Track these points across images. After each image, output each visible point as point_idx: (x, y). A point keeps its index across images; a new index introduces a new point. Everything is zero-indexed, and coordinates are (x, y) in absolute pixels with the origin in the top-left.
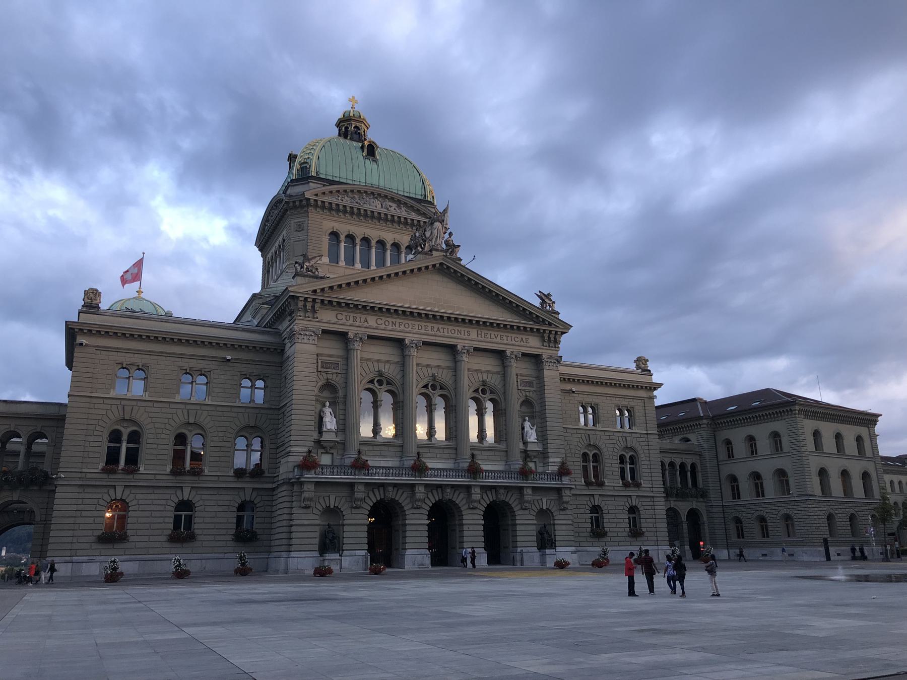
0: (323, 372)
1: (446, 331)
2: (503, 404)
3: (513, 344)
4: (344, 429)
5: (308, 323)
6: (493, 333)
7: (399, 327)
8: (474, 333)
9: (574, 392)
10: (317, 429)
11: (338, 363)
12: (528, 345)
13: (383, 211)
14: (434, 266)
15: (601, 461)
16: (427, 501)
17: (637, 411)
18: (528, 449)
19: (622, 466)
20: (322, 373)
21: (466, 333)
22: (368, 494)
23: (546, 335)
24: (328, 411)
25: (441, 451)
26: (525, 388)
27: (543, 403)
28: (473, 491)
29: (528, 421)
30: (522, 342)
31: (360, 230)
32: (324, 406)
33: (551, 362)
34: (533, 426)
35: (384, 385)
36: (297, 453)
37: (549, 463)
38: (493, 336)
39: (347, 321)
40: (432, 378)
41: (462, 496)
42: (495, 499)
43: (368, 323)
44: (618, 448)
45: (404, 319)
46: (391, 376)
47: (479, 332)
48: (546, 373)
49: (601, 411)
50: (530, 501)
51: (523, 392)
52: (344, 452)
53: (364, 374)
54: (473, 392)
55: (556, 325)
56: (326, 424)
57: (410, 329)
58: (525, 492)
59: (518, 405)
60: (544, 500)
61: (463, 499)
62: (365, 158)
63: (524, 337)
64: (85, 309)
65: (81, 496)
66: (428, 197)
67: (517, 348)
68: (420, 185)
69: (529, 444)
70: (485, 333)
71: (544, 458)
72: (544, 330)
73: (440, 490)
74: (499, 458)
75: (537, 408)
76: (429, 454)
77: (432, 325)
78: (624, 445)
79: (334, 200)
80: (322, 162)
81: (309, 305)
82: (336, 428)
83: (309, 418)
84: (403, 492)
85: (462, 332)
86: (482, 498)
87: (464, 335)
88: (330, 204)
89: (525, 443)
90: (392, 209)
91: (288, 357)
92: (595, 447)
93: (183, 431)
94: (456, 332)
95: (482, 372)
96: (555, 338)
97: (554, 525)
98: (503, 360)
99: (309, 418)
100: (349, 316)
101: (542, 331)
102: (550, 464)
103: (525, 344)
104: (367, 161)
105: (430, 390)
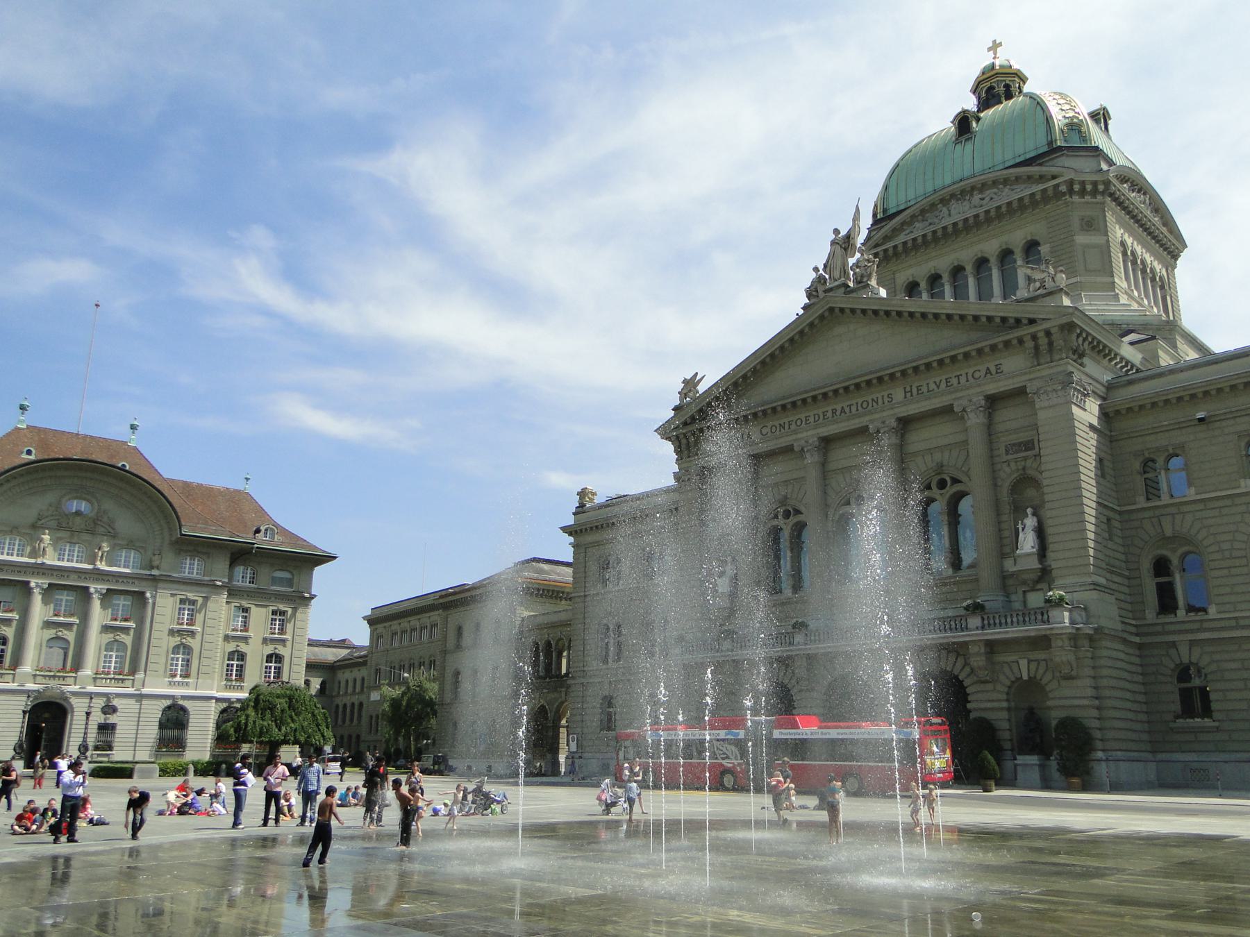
1: (854, 408)
8: (898, 394)
9: (1201, 420)
14: (822, 317)
21: (885, 397)
23: (1030, 344)
29: (1034, 514)
38: (932, 386)
47: (908, 389)
48: (1042, 415)
51: (1012, 464)
55: (1044, 319)
66: (1056, 140)
67: (978, 390)
68: (1042, 129)
70: (917, 387)
72: (1021, 341)
77: (835, 407)
79: (902, 238)
80: (892, 190)
81: (684, 441)
85: (880, 401)
88: (895, 247)
90: (984, 202)
94: (870, 405)
101: (1015, 342)
104: (959, 147)
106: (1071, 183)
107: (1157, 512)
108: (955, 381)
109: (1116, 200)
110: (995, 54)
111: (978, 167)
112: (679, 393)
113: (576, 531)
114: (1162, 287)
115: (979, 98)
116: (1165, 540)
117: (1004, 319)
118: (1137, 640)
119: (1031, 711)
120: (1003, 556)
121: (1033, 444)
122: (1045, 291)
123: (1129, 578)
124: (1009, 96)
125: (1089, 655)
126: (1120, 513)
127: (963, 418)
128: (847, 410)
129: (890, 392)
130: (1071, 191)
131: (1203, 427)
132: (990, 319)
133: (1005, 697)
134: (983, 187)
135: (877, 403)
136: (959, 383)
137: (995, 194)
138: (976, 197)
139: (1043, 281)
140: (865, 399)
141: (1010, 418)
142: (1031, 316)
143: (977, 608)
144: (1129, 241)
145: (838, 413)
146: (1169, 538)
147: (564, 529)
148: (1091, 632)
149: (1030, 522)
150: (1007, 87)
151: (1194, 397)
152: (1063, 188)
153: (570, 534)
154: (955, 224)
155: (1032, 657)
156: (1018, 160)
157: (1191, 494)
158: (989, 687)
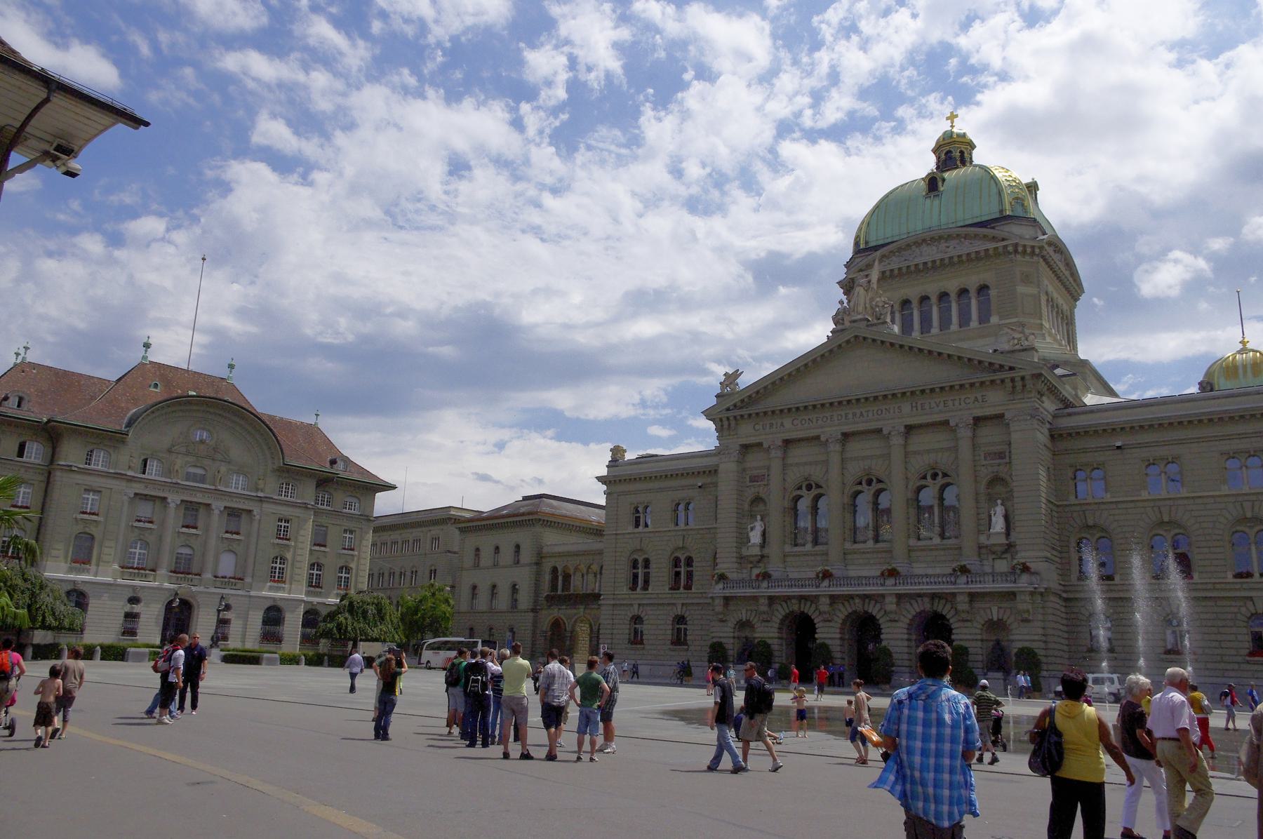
1: (870, 414)
3: (961, 410)
8: (906, 408)
9: (1119, 448)
13: (938, 257)
14: (848, 342)
23: (1009, 384)
26: (994, 462)
29: (1002, 504)
31: (932, 287)
38: (933, 405)
39: (763, 429)
43: (784, 426)
47: (914, 404)
48: (1015, 437)
60: (995, 610)
62: (927, 196)
64: (612, 464)
65: (615, 612)
72: (1003, 381)
81: (726, 423)
85: (892, 411)
87: (894, 412)
90: (949, 250)
92: (1172, 523)
93: (676, 555)
95: (929, 451)
97: (1013, 641)
101: (998, 382)
104: (928, 201)
106: (1016, 245)
107: (1084, 508)
108: (950, 403)
109: (1045, 260)
110: (952, 123)
111: (943, 220)
112: (721, 383)
113: (610, 482)
114: (1067, 324)
115: (938, 158)
116: (1088, 527)
117: (991, 364)
118: (1064, 595)
119: (998, 642)
120: (979, 532)
121: (1005, 456)
122: (1021, 348)
123: (1061, 552)
124: (963, 163)
125: (1041, 605)
126: (1058, 506)
127: (955, 431)
128: (865, 414)
130: (1016, 251)
131: (1118, 451)
132: (980, 362)
134: (949, 237)
137: (958, 244)
138: (943, 245)
139: (1019, 339)
141: (989, 435)
142: (1012, 365)
143: (964, 570)
144: (1050, 289)
145: (858, 415)
146: (1091, 527)
147: (599, 479)
148: (1043, 590)
149: (1000, 510)
150: (962, 153)
151: (1113, 430)
152: (1010, 249)
153: (604, 483)
154: (925, 264)
155: (1000, 605)
156: (979, 220)
157: (1108, 497)
158: (969, 624)
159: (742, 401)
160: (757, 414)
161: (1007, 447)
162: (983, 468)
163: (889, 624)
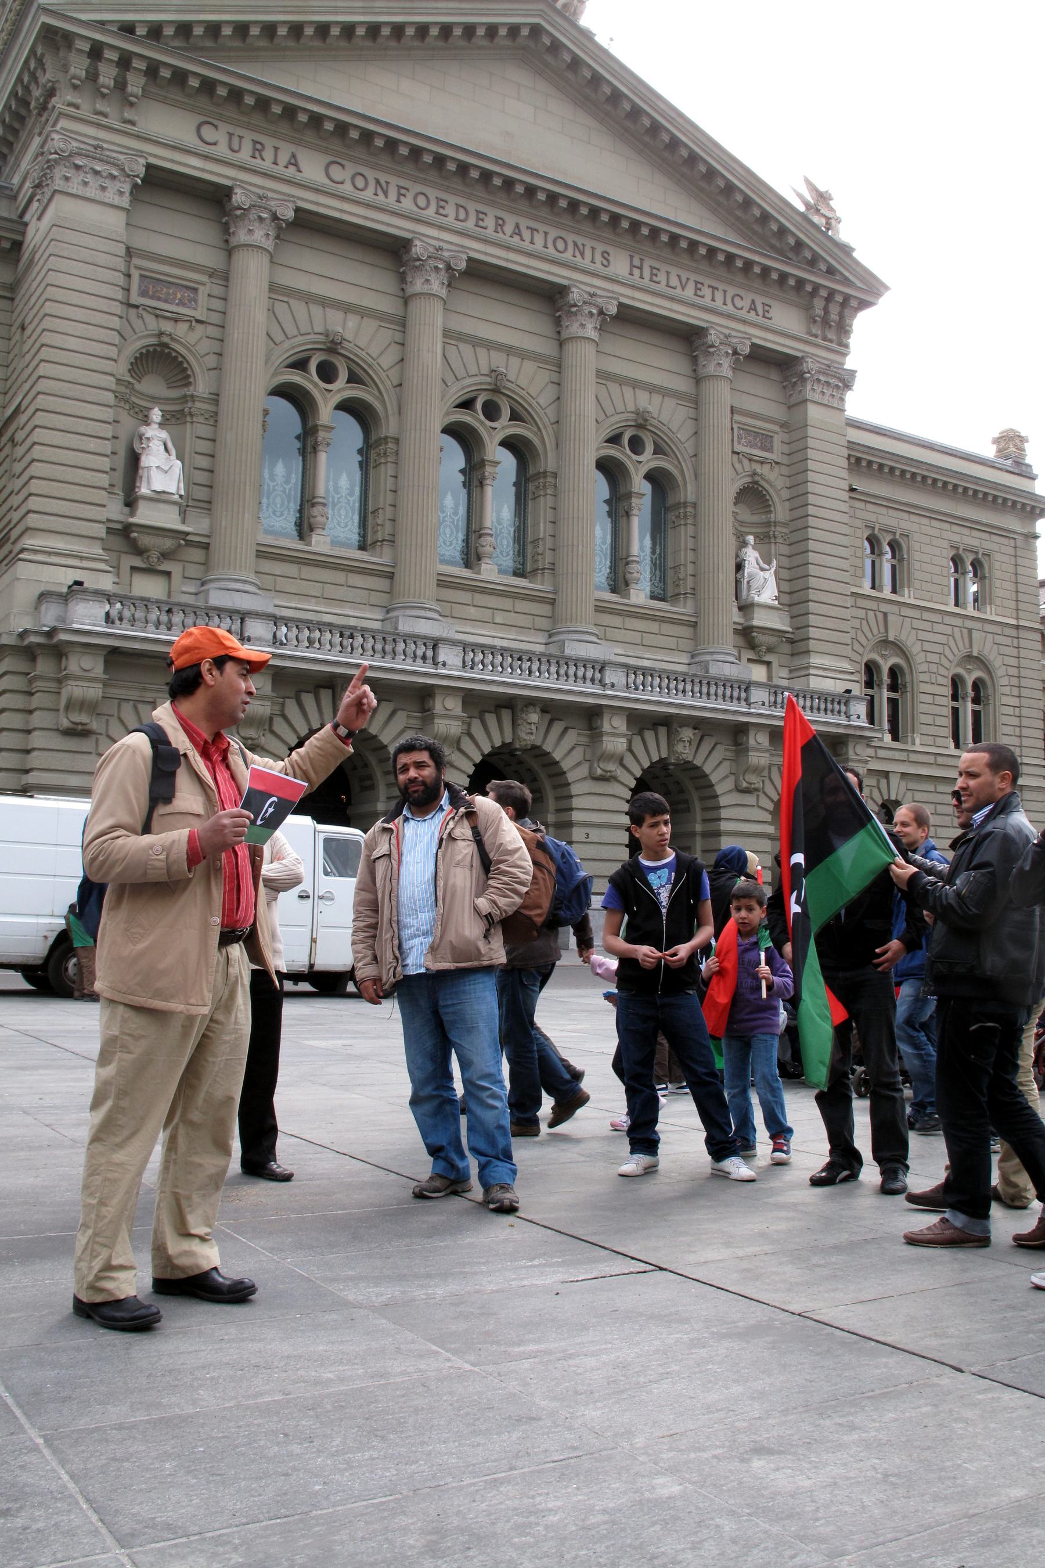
0: (146, 308)
1: (539, 239)
2: (690, 488)
4: (210, 502)
5: (102, 134)
6: (674, 272)
7: (398, 201)
10: (118, 490)
11: (196, 290)
12: (768, 322)
14: (514, 30)
15: (909, 686)
16: (467, 745)
17: (997, 565)
18: (755, 623)
19: (955, 704)
20: (140, 310)
22: (282, 711)
24: (156, 435)
25: (506, 603)
27: (799, 498)
28: (606, 727)
29: (754, 548)
30: (753, 313)
32: (146, 421)
33: (828, 383)
34: (769, 563)
35: (341, 382)
36: (50, 554)
37: (808, 668)
38: (674, 281)
39: (234, 151)
40: (488, 379)
41: (572, 737)
42: (664, 755)
43: (299, 171)
44: (951, 657)
45: (416, 180)
46: (362, 354)
49: (916, 556)
50: (763, 769)
51: (746, 462)
52: (207, 571)
53: (279, 337)
54: (606, 442)
55: (846, 279)
56: (149, 478)
57: (431, 212)
58: (752, 742)
59: (732, 500)
61: (573, 748)
63: (759, 301)
69: (756, 610)
71: (792, 655)
73: (506, 715)
74: (671, 642)
75: (781, 512)
76: (472, 610)
78: (964, 651)
81: (107, 75)
82: (182, 493)
83: (92, 445)
84: (393, 713)
85: (588, 253)
86: (630, 749)
87: (593, 262)
89: (746, 608)
91: (34, 252)
96: (841, 316)
98: (694, 360)
99: (92, 445)
100: (241, 137)
101: (809, 288)
102: (812, 671)
103: (760, 320)
105: (482, 417)
108: (707, 292)
121: (771, 442)
128: (526, 234)
129: (609, 249)
133: (768, 817)
135: (582, 254)
136: (713, 300)
140: (564, 234)
145: (509, 228)
158: (750, 799)
159: (184, 29)
160: (236, 95)
161: (776, 428)
162: (735, 456)
163: (589, 786)
